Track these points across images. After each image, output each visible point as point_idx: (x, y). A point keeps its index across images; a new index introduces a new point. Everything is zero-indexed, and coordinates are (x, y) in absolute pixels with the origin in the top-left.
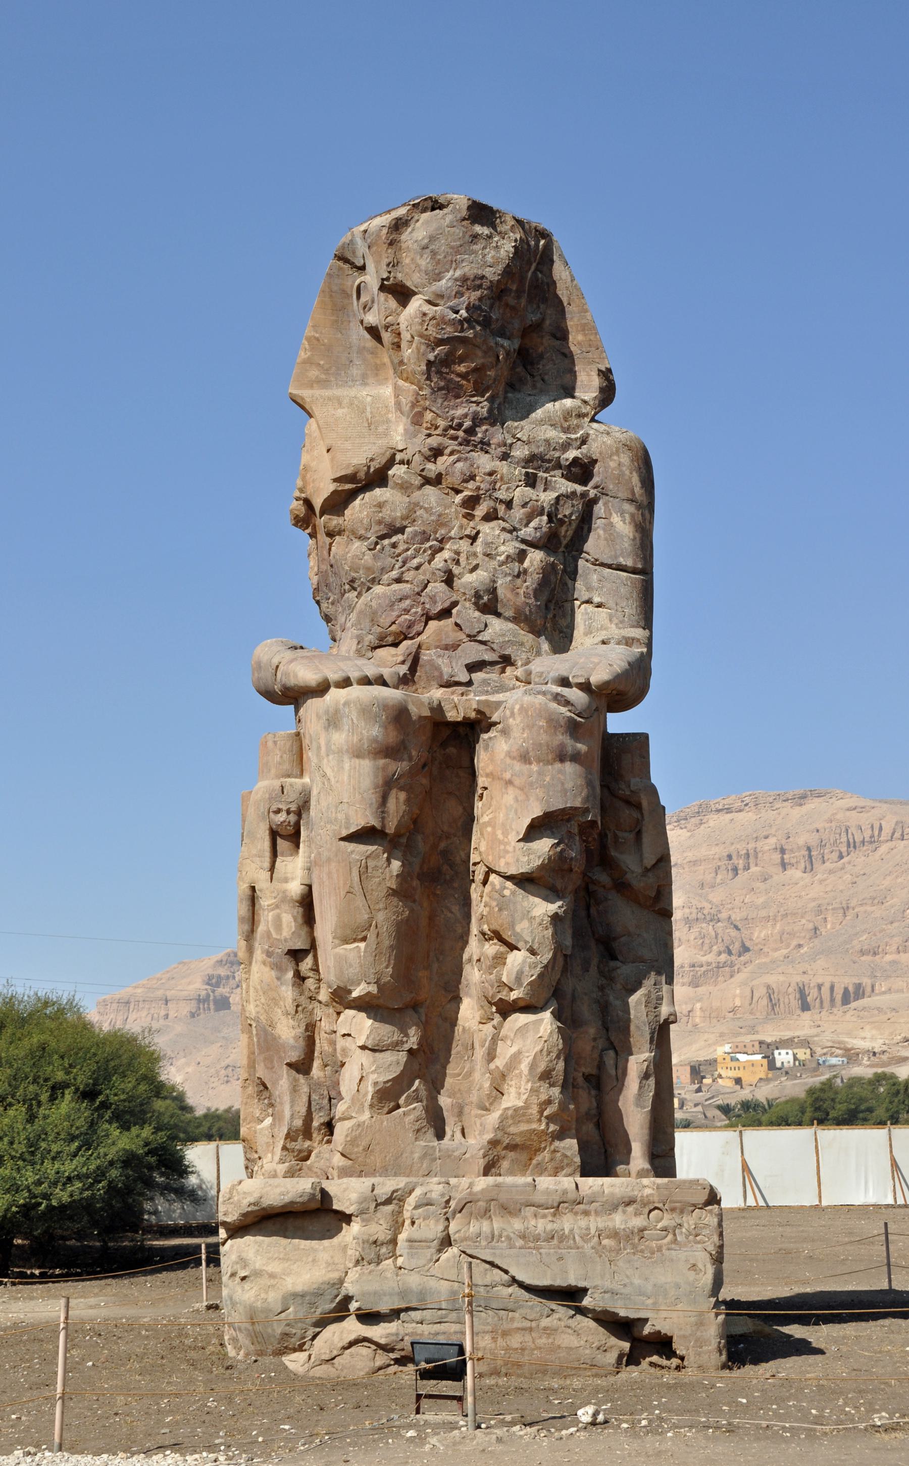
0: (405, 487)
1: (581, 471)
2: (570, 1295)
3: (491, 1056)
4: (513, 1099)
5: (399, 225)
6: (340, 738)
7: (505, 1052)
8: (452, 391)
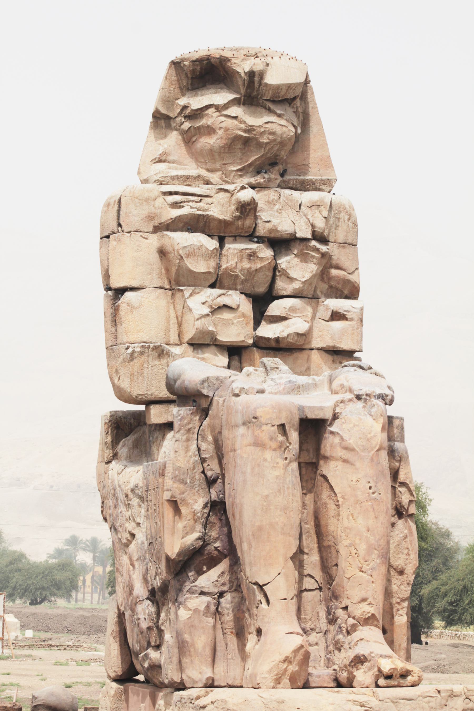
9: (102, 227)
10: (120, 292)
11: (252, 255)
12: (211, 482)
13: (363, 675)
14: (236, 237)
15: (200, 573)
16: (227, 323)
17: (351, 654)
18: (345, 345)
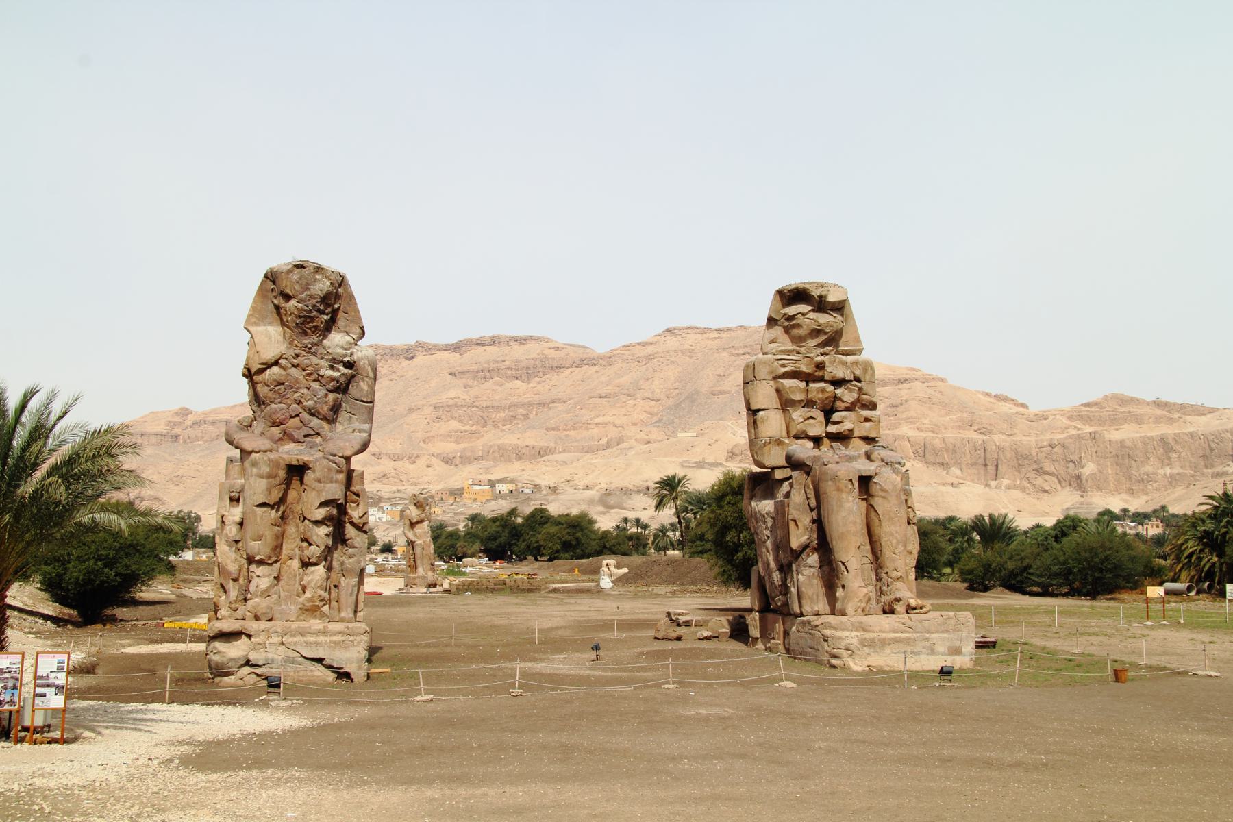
0: (285, 369)
1: (349, 365)
2: (319, 661)
3: (302, 579)
4: (308, 594)
5: (290, 271)
6: (255, 470)
7: (306, 579)
8: (305, 334)
9: (744, 378)
10: (756, 411)
11: (823, 390)
12: (812, 510)
13: (899, 607)
14: (814, 381)
15: (808, 556)
16: (812, 425)
17: (892, 597)
18: (872, 435)
